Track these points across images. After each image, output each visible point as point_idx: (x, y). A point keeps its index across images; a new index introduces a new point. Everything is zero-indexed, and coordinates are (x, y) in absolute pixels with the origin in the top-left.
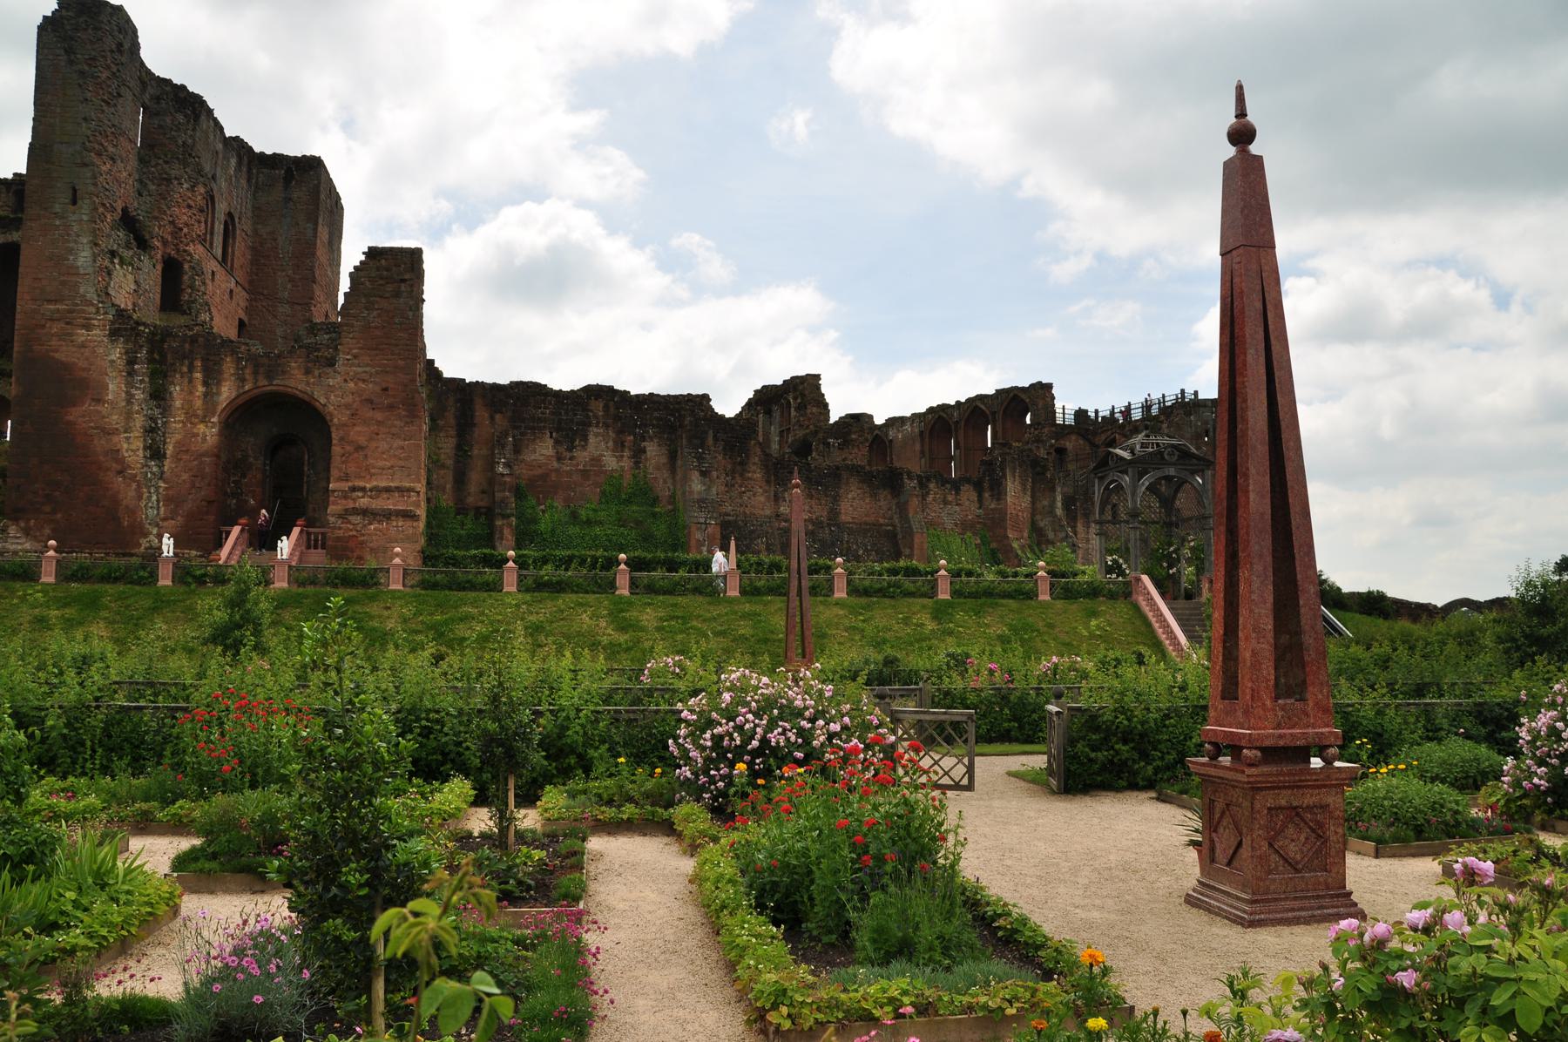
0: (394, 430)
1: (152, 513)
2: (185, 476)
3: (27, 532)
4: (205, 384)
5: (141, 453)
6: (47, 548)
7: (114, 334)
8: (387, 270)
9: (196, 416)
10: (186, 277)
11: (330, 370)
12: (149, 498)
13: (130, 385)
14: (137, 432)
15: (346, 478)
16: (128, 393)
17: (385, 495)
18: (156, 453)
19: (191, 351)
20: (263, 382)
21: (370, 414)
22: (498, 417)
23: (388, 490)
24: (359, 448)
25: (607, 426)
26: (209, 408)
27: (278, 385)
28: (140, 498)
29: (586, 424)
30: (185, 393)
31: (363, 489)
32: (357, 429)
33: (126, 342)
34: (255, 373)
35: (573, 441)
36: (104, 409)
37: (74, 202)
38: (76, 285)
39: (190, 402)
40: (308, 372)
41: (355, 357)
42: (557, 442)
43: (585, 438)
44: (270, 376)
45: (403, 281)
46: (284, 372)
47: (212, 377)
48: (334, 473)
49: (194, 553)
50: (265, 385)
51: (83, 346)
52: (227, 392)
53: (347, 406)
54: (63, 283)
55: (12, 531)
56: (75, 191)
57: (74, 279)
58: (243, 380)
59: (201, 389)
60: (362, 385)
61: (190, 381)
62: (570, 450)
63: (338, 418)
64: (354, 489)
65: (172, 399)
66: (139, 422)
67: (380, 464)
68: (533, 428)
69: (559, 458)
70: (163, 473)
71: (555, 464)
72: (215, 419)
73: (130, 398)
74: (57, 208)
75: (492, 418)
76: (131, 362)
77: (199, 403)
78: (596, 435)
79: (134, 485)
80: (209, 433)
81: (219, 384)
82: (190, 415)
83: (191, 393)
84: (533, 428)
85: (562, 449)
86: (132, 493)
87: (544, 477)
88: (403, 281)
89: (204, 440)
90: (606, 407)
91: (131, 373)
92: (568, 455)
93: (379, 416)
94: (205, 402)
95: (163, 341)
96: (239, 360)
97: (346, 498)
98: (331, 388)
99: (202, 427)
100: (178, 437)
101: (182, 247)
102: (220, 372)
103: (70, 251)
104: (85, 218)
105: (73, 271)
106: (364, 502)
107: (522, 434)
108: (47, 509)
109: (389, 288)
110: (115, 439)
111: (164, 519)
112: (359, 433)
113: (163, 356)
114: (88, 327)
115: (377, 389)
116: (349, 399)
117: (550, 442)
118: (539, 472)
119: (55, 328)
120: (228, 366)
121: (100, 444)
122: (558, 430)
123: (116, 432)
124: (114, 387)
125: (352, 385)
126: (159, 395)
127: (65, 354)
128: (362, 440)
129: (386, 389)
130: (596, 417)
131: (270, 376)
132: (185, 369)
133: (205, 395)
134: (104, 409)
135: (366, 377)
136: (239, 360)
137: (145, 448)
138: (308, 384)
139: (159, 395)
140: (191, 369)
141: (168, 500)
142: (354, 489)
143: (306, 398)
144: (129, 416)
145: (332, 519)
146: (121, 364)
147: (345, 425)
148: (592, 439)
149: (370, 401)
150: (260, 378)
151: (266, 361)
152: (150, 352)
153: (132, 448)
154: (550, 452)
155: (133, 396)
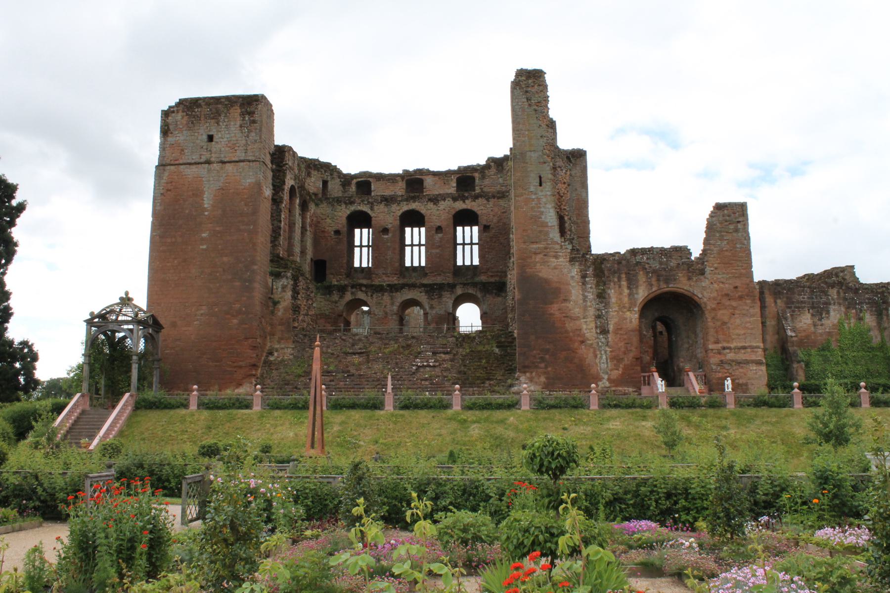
0: (744, 312)
1: (604, 366)
2: (622, 344)
3: (531, 380)
4: (629, 288)
5: (594, 330)
6: (256, 390)
7: (572, 260)
8: (729, 216)
9: (624, 307)
10: (567, 225)
11: (702, 277)
12: (601, 357)
13: (584, 290)
14: (591, 319)
15: (717, 342)
16: (583, 295)
17: (743, 351)
18: (604, 331)
19: (619, 269)
20: (663, 285)
21: (728, 303)
22: (779, 301)
23: (744, 348)
24: (724, 323)
25: (840, 304)
26: (632, 304)
27: (672, 287)
28: (596, 356)
29: (827, 304)
30: (617, 294)
31: (729, 348)
32: (721, 312)
33: (581, 264)
34: (658, 280)
35: (821, 314)
36: (570, 305)
37: (541, 185)
38: (547, 234)
39: (620, 299)
40: (689, 279)
41: (716, 268)
42: (812, 315)
43: (828, 312)
44: (667, 281)
45: (739, 222)
46: (675, 280)
47: (632, 283)
48: (712, 339)
49: (631, 389)
50: (665, 288)
51: (555, 268)
52: (642, 294)
53: (714, 299)
54: (540, 232)
55: (523, 379)
56: (540, 177)
57: (546, 229)
58: (651, 285)
59: (626, 291)
60: (722, 285)
61: (620, 287)
62: (820, 320)
63: (711, 305)
64: (724, 348)
65: (610, 297)
66: (591, 312)
67: (737, 331)
68: (798, 308)
69: (815, 325)
70: (608, 342)
71: (812, 329)
72: (636, 309)
73: (585, 298)
74: (532, 189)
75: (775, 302)
76: (584, 277)
77: (626, 300)
78: (834, 310)
79: (592, 350)
80: (633, 317)
81: (637, 287)
82: (622, 307)
83: (621, 294)
84: (798, 308)
85: (816, 319)
86: (591, 355)
87: (807, 337)
88: (739, 222)
89: (631, 322)
90: (838, 292)
91: (584, 283)
92: (819, 323)
93: (734, 304)
94: (630, 299)
95: (602, 263)
96: (648, 273)
97: (720, 353)
98: (704, 288)
99: (628, 313)
100: (616, 320)
101: (563, 207)
102: (637, 281)
103: (542, 213)
104: (549, 193)
105: (544, 225)
106: (730, 356)
107: (793, 311)
108: (542, 365)
109: (732, 227)
110: (577, 322)
111: (611, 370)
112: (723, 314)
113: (602, 272)
114: (556, 257)
115: (732, 287)
116: (715, 294)
117: (809, 316)
118: (803, 334)
119: (538, 258)
120: (642, 278)
121: (570, 326)
122: (813, 308)
123: (577, 318)
124: (575, 292)
125: (716, 286)
126: (602, 296)
127: (544, 273)
128: (726, 319)
129: (736, 287)
130: (833, 299)
131: (667, 281)
132: (616, 280)
133: (629, 295)
134: (570, 305)
135: (722, 280)
136: (648, 273)
137: (596, 327)
138: (690, 286)
139: (602, 296)
140: (619, 279)
141: (613, 358)
142: (724, 348)
143: (689, 294)
144: (585, 309)
145: (714, 367)
146: (578, 277)
147: (714, 309)
148: (832, 313)
149: (727, 295)
150: (661, 283)
151: (664, 273)
152: (595, 270)
153: (588, 328)
154: (809, 321)
155: (586, 297)
